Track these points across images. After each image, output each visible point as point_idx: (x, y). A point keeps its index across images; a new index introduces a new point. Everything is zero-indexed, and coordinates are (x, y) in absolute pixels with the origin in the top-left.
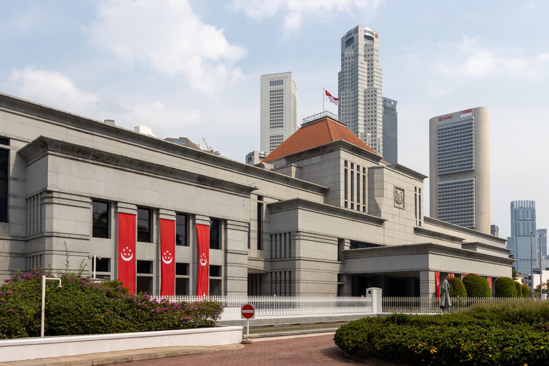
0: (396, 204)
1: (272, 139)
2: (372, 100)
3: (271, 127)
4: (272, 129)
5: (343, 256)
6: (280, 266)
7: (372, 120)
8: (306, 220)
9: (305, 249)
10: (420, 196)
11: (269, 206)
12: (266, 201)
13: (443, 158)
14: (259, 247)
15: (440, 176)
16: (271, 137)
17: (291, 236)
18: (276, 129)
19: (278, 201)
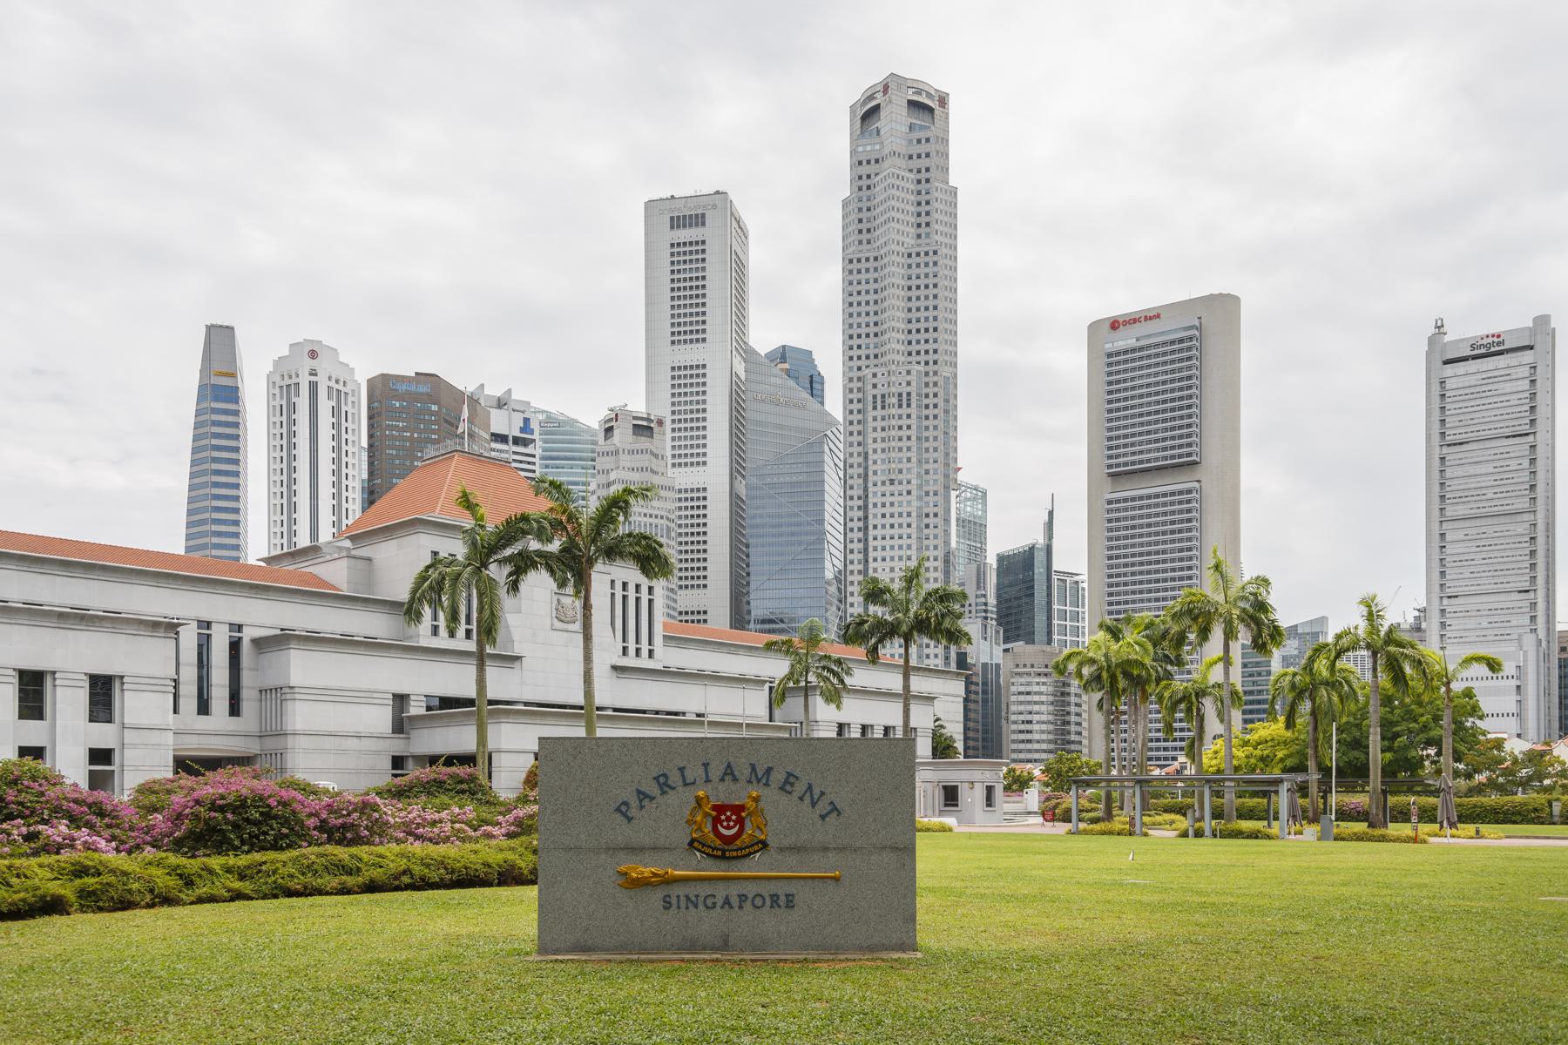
0: (558, 625)
1: (676, 373)
2: (927, 276)
3: (673, 342)
4: (676, 347)
5: (401, 725)
6: (270, 744)
7: (927, 330)
8: (301, 667)
9: (300, 716)
10: (650, 601)
11: (259, 643)
12: (248, 634)
13: (1118, 428)
14: (235, 710)
15: (1111, 475)
16: (673, 369)
17: (277, 694)
18: (688, 346)
19: (278, 632)
